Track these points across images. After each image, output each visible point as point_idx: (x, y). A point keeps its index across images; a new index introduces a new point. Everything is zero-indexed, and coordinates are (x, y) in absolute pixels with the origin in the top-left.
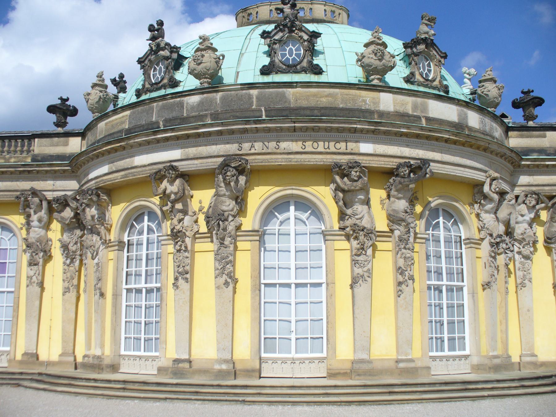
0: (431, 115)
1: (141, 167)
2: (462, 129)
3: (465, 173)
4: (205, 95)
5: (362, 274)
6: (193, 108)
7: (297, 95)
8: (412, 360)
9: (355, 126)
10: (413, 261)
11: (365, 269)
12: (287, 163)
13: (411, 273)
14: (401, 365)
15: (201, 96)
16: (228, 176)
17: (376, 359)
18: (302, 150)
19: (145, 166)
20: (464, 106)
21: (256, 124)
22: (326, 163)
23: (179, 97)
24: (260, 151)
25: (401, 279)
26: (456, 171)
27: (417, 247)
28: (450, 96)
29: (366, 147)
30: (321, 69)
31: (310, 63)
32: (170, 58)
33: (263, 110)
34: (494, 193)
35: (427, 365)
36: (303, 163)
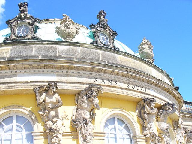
1: (23, 83)
4: (71, 47)
6: (62, 52)
7: (121, 58)
9: (151, 80)
12: (122, 94)
15: (69, 47)
16: (93, 96)
18: (128, 88)
19: (27, 82)
21: (109, 68)
22: (139, 97)
23: (53, 44)
24: (107, 84)
31: (114, 47)
32: (34, 25)
33: (107, 62)
36: (129, 95)
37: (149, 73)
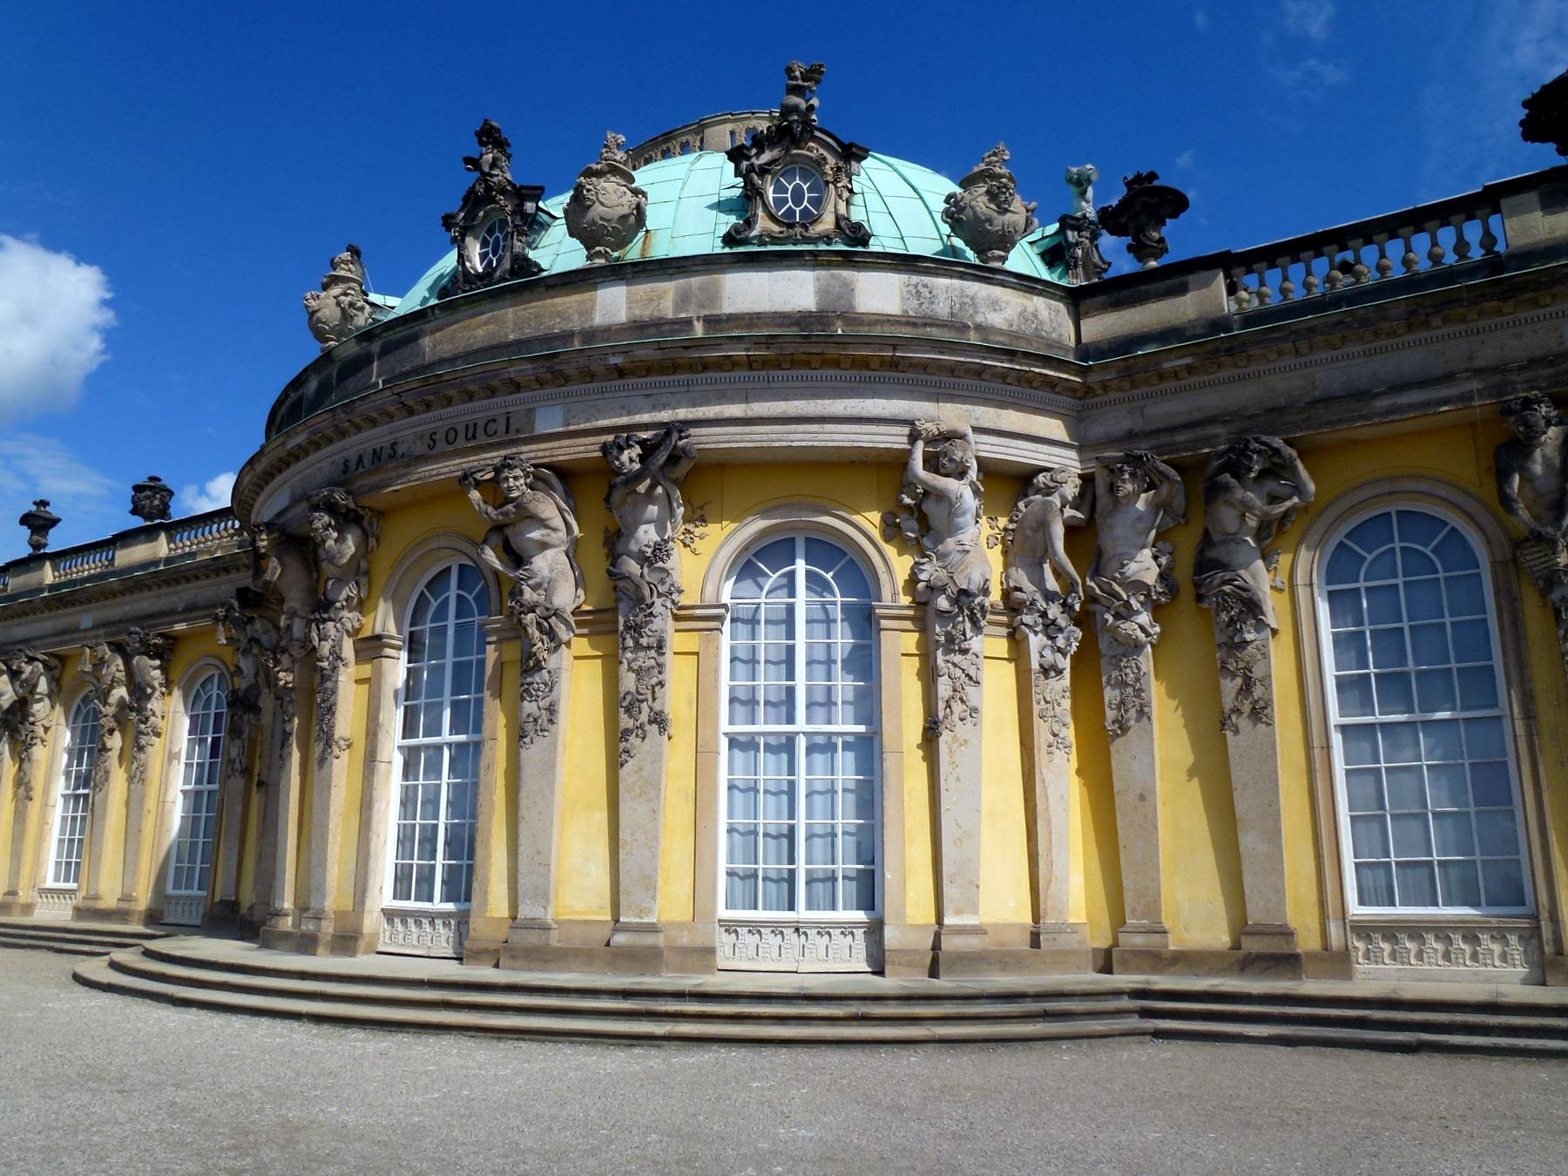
0: (727, 308)
2: (823, 324)
3: (821, 437)
5: (537, 713)
8: (652, 929)
10: (661, 677)
11: (544, 703)
13: (657, 706)
14: (620, 939)
17: (570, 921)
20: (839, 266)
25: (626, 722)
26: (792, 437)
27: (677, 641)
28: (872, 249)
29: (548, 421)
30: (536, 265)
34: (947, 476)
35: (708, 944)
37: (568, 326)
